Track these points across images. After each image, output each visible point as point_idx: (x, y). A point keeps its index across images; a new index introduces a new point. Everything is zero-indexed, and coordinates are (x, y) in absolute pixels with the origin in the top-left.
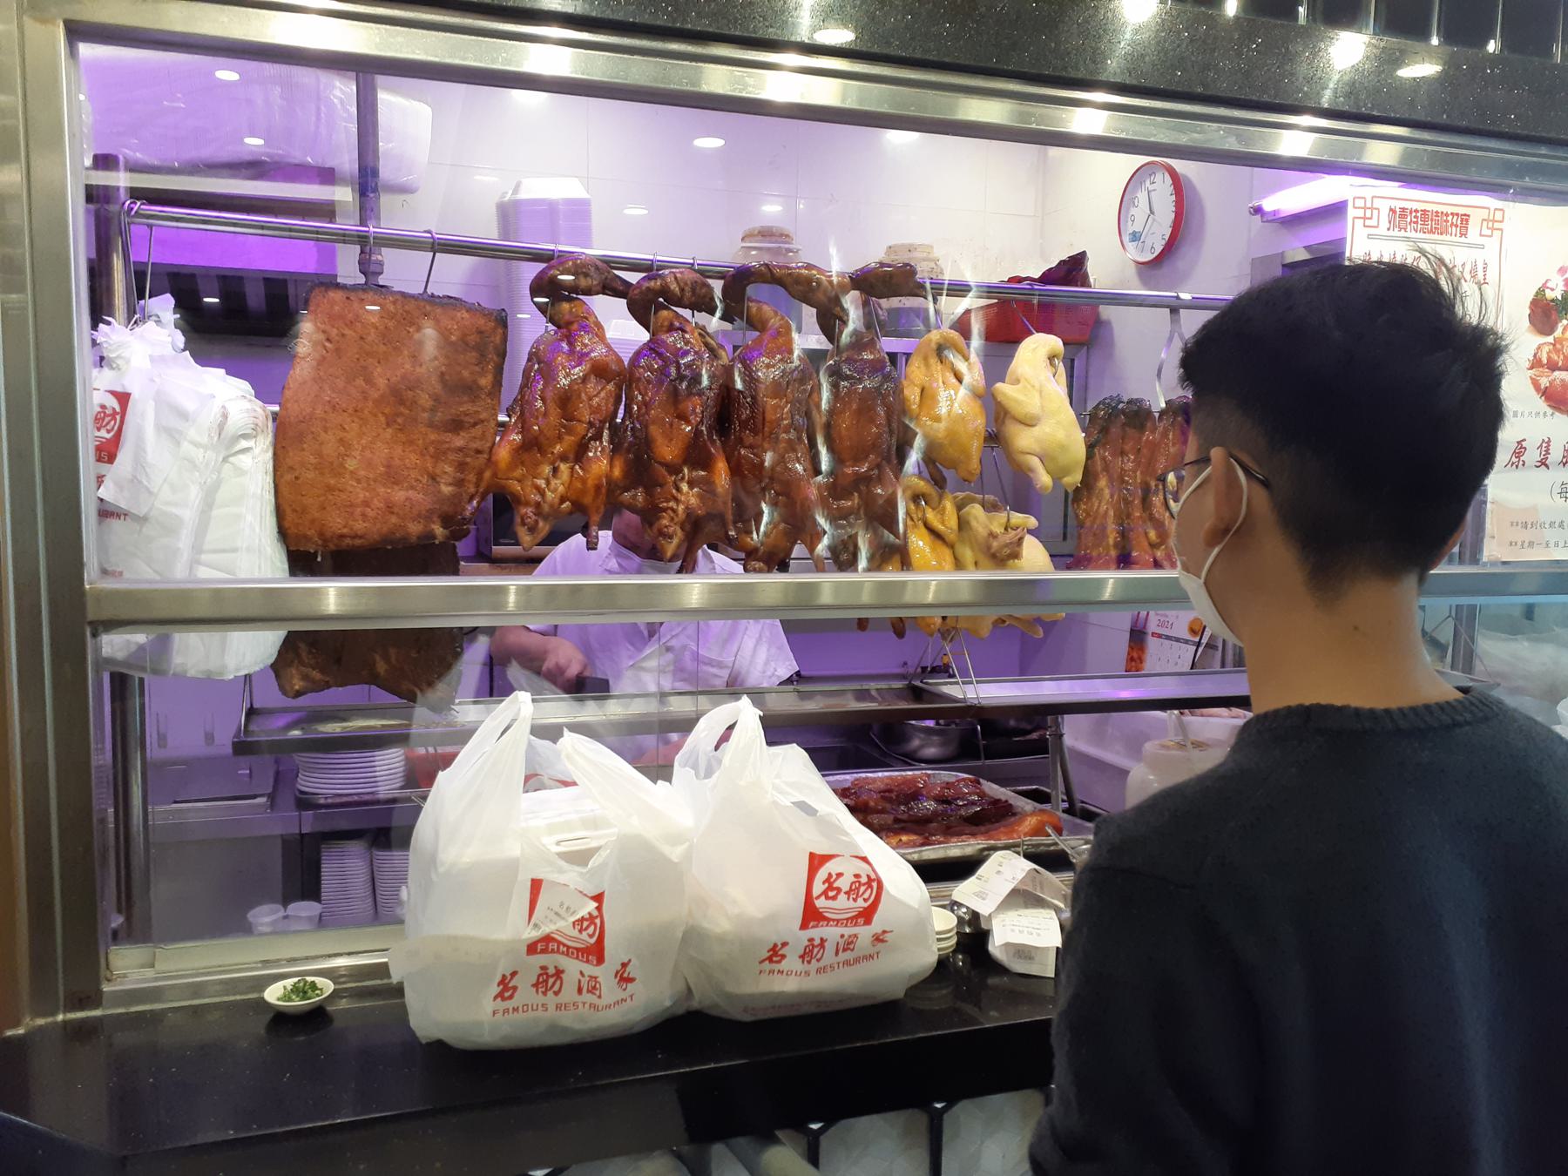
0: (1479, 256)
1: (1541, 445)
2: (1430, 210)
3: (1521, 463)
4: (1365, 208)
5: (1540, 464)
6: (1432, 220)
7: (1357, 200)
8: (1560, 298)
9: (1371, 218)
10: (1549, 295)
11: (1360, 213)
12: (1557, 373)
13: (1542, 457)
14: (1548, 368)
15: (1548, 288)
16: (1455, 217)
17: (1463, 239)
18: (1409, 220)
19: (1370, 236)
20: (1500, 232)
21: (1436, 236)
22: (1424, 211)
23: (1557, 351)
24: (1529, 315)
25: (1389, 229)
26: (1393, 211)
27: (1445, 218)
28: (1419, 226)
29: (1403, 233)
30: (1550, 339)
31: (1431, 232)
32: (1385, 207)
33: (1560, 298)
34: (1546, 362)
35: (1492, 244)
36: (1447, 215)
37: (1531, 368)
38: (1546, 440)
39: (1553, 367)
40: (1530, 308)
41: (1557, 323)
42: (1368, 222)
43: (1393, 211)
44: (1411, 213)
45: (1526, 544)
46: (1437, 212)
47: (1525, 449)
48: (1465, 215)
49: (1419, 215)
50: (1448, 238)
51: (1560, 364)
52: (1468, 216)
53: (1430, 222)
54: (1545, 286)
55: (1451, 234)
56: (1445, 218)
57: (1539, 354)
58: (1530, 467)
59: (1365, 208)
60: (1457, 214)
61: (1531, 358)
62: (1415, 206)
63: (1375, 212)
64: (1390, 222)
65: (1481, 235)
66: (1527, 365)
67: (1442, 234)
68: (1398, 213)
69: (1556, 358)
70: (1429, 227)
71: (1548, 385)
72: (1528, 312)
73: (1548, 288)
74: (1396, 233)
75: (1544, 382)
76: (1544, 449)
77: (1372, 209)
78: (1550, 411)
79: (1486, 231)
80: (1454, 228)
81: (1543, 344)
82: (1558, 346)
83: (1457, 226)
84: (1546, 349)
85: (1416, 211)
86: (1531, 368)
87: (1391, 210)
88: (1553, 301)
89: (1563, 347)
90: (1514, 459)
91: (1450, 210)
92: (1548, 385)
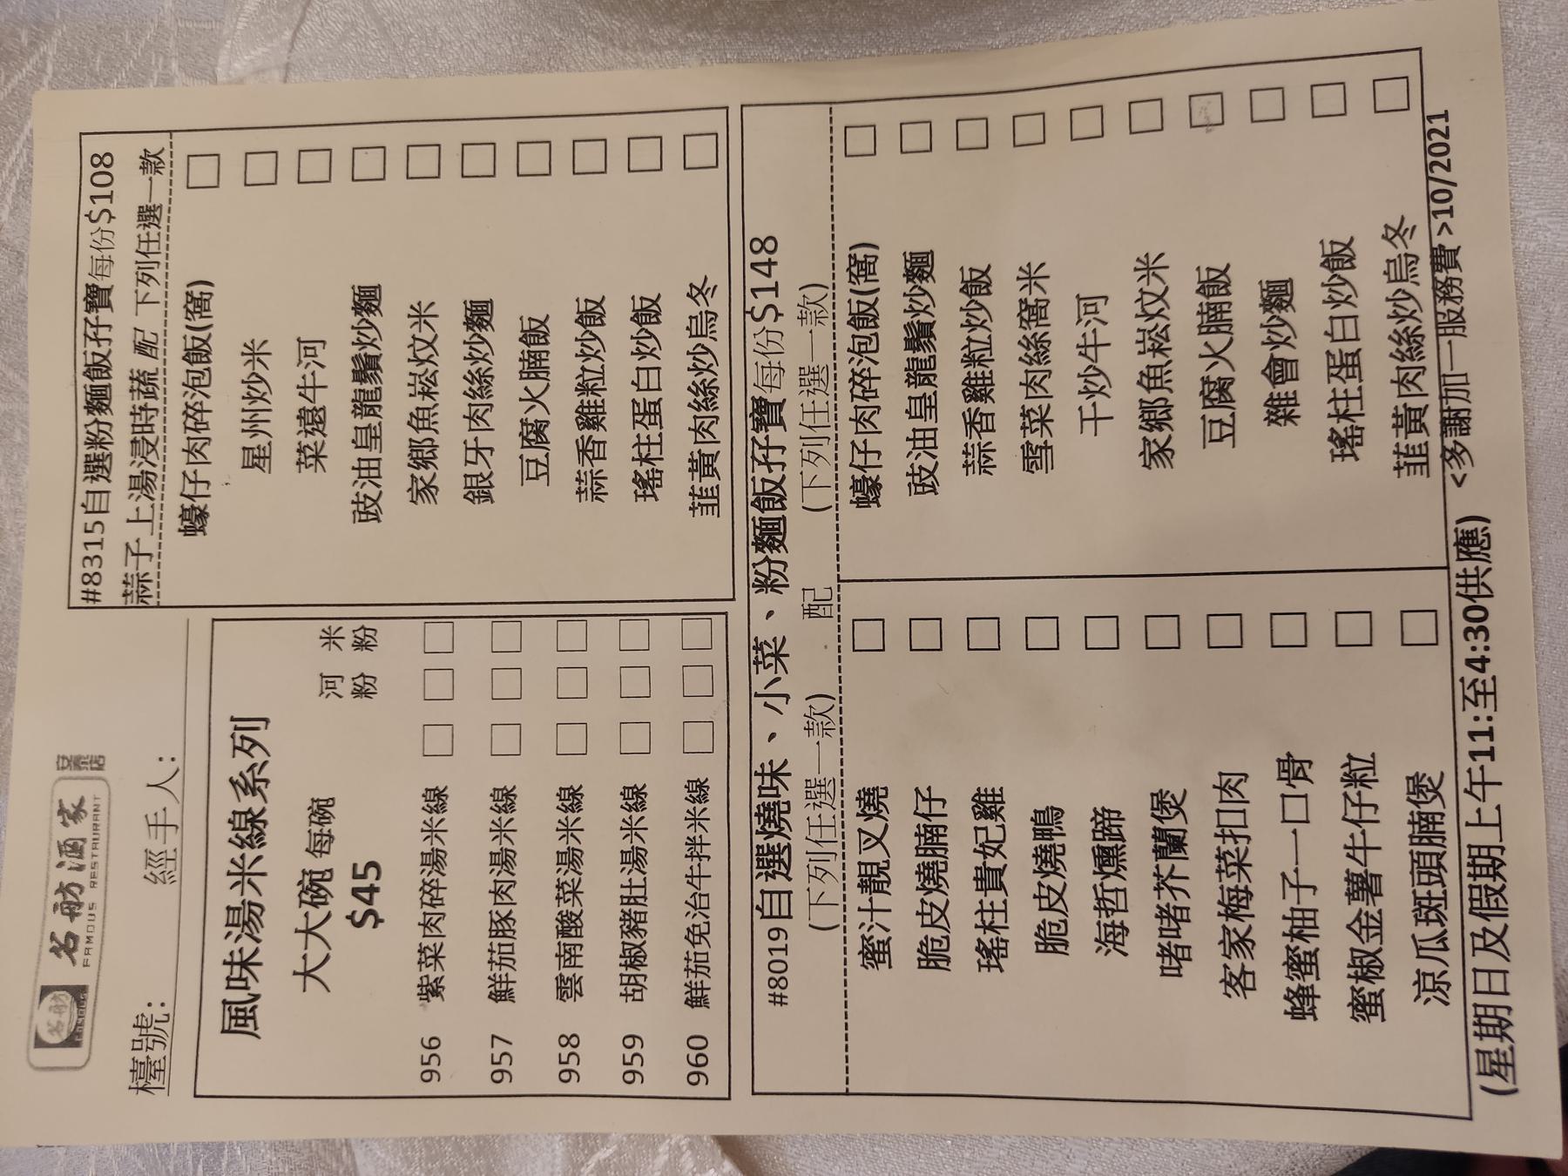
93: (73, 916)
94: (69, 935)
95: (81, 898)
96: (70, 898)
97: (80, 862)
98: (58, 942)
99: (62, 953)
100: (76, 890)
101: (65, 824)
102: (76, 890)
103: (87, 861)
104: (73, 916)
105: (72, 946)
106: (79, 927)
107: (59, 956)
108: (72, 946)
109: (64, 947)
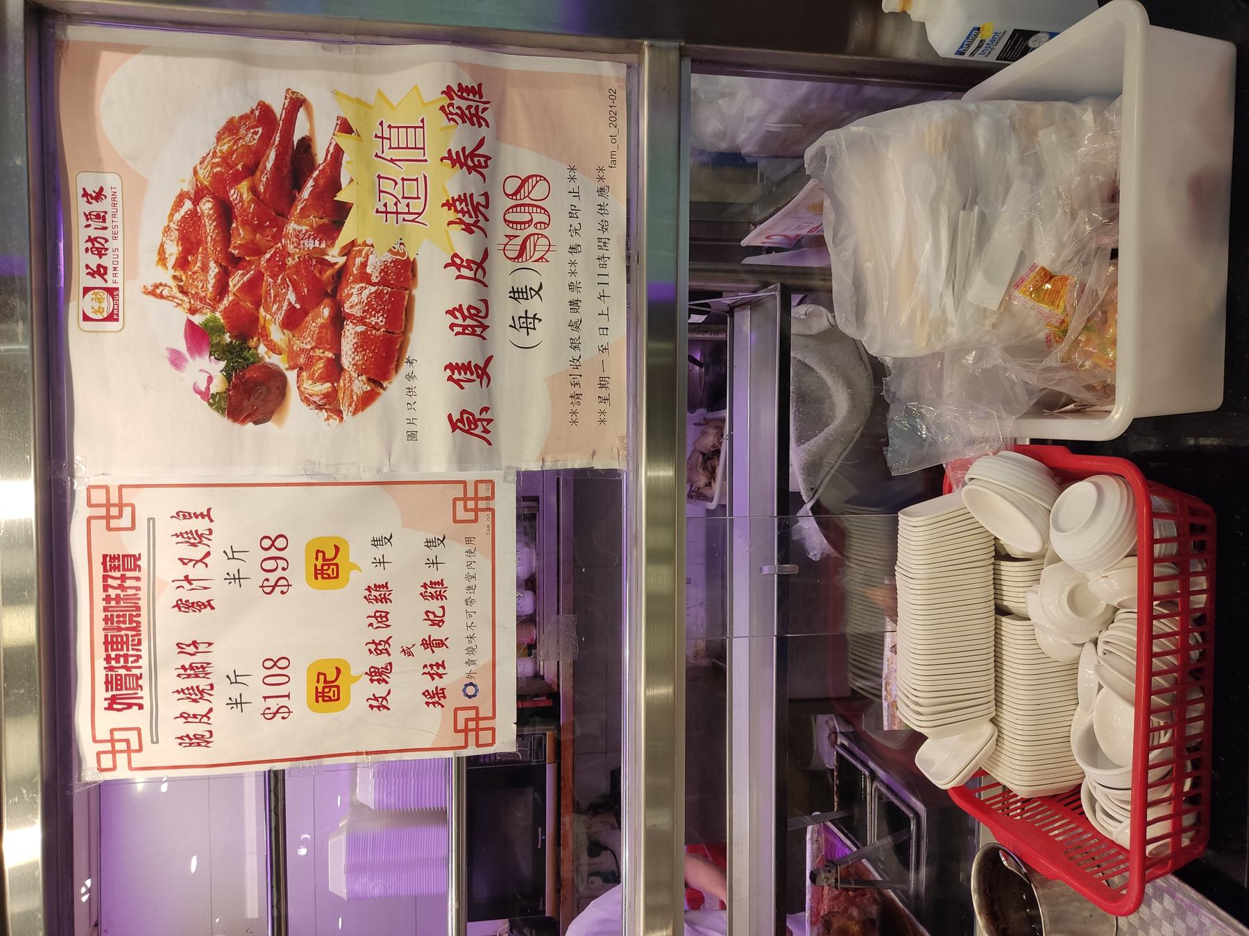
0: (168, 527)
1: (457, 382)
2: (103, 633)
3: (484, 416)
4: (114, 752)
5: (485, 378)
6: (120, 629)
7: (104, 766)
8: (223, 364)
9: (127, 741)
10: (218, 386)
11: (122, 759)
12: (346, 362)
13: (474, 377)
14: (338, 381)
15: (208, 388)
16: (110, 582)
17: (143, 563)
18: (123, 672)
19: (154, 740)
20: (124, 490)
21: (143, 619)
22: (106, 643)
23: (311, 361)
24: (256, 423)
25: (141, 707)
26: (112, 704)
27: (113, 603)
28: (131, 652)
29: (144, 682)
30: (291, 376)
31: (136, 629)
32: (108, 720)
33: (223, 364)
34: (328, 385)
35: (146, 504)
36: (108, 599)
37: (339, 413)
38: (449, 372)
39: (334, 370)
40: (243, 422)
41: (265, 366)
42: (134, 745)
43: (112, 704)
44: (111, 669)
45: (603, 393)
46: (106, 619)
47: (464, 412)
48: (104, 563)
49: (113, 654)
50: (143, 594)
51: (330, 355)
52: (105, 556)
53: (123, 633)
54: (205, 395)
55: (138, 589)
56: (113, 603)
57: (316, 399)
58: (490, 396)
59: (114, 752)
60: (105, 578)
61: (324, 414)
62: (101, 664)
63: (117, 735)
64: (130, 706)
65: (133, 528)
66: (334, 422)
67: (138, 609)
68: (115, 692)
69: (321, 364)
70: (130, 633)
71: (364, 378)
72: (250, 425)
73: (208, 388)
74: (144, 693)
75: (360, 385)
76: (462, 377)
77: (113, 741)
78: (405, 368)
79: (125, 521)
80: (128, 583)
81: (301, 393)
82: (302, 360)
83: (123, 578)
84: (307, 384)
85: (108, 659)
86: (339, 413)
87: (110, 708)
88: (228, 378)
89: (303, 350)
90: (478, 431)
91: (99, 594)
92: (364, 378)
93: (100, 255)
94: (99, 266)
95: (106, 245)
96: (97, 245)
97: (104, 225)
98: (91, 269)
99: (96, 275)
100: (103, 241)
101: (88, 202)
102: (103, 241)
103: (108, 224)
104: (100, 255)
105: (102, 272)
106: (105, 261)
107: (95, 277)
108: (102, 272)
109: (98, 272)
